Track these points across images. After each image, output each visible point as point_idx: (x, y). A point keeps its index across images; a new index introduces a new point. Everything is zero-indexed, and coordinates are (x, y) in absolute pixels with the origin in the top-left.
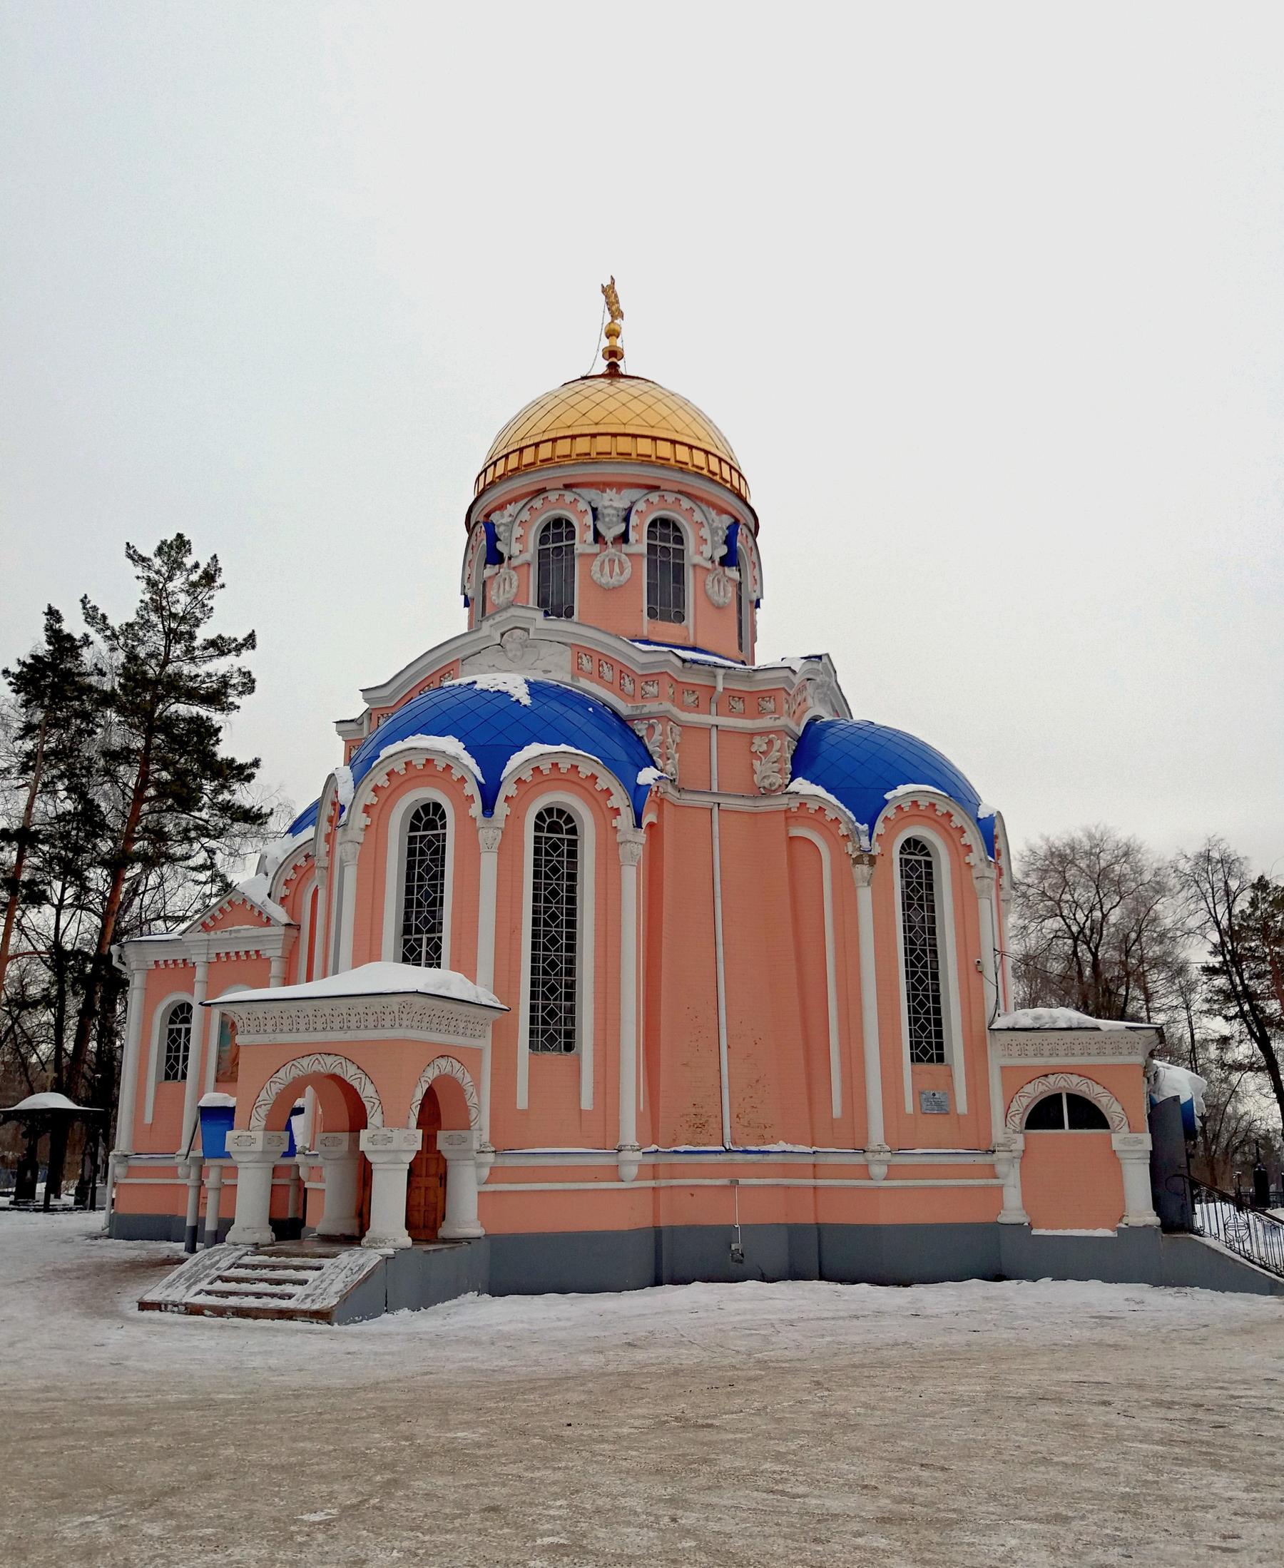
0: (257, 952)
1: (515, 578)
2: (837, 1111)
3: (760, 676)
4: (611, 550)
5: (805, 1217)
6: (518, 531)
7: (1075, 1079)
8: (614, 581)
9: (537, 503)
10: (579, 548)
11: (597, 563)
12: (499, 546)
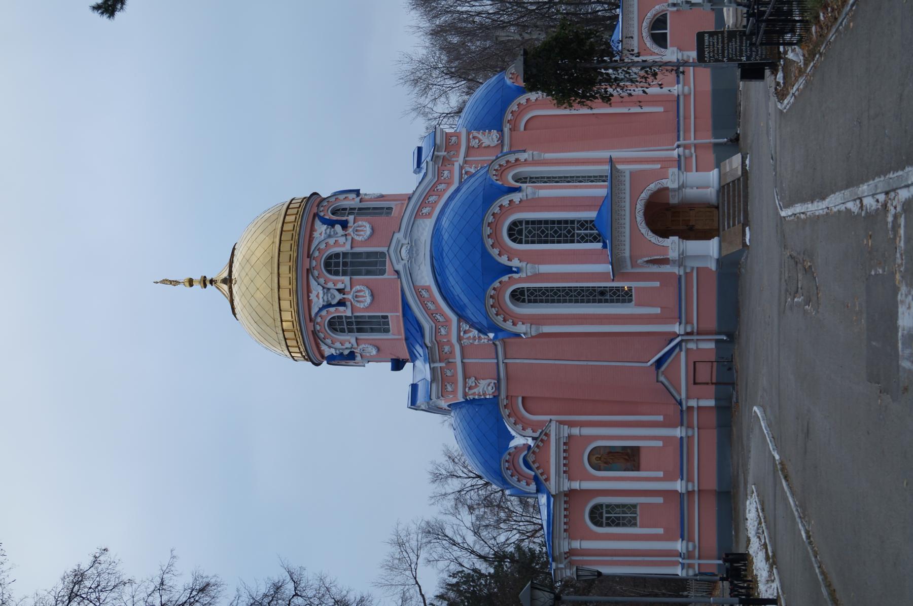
0: (565, 444)
1: (358, 288)
2: (661, 109)
3: (438, 141)
4: (350, 230)
5: (709, 121)
6: (330, 285)
7: (644, 24)
8: (368, 231)
9: (316, 273)
10: (347, 248)
11: (356, 238)
12: (334, 302)
